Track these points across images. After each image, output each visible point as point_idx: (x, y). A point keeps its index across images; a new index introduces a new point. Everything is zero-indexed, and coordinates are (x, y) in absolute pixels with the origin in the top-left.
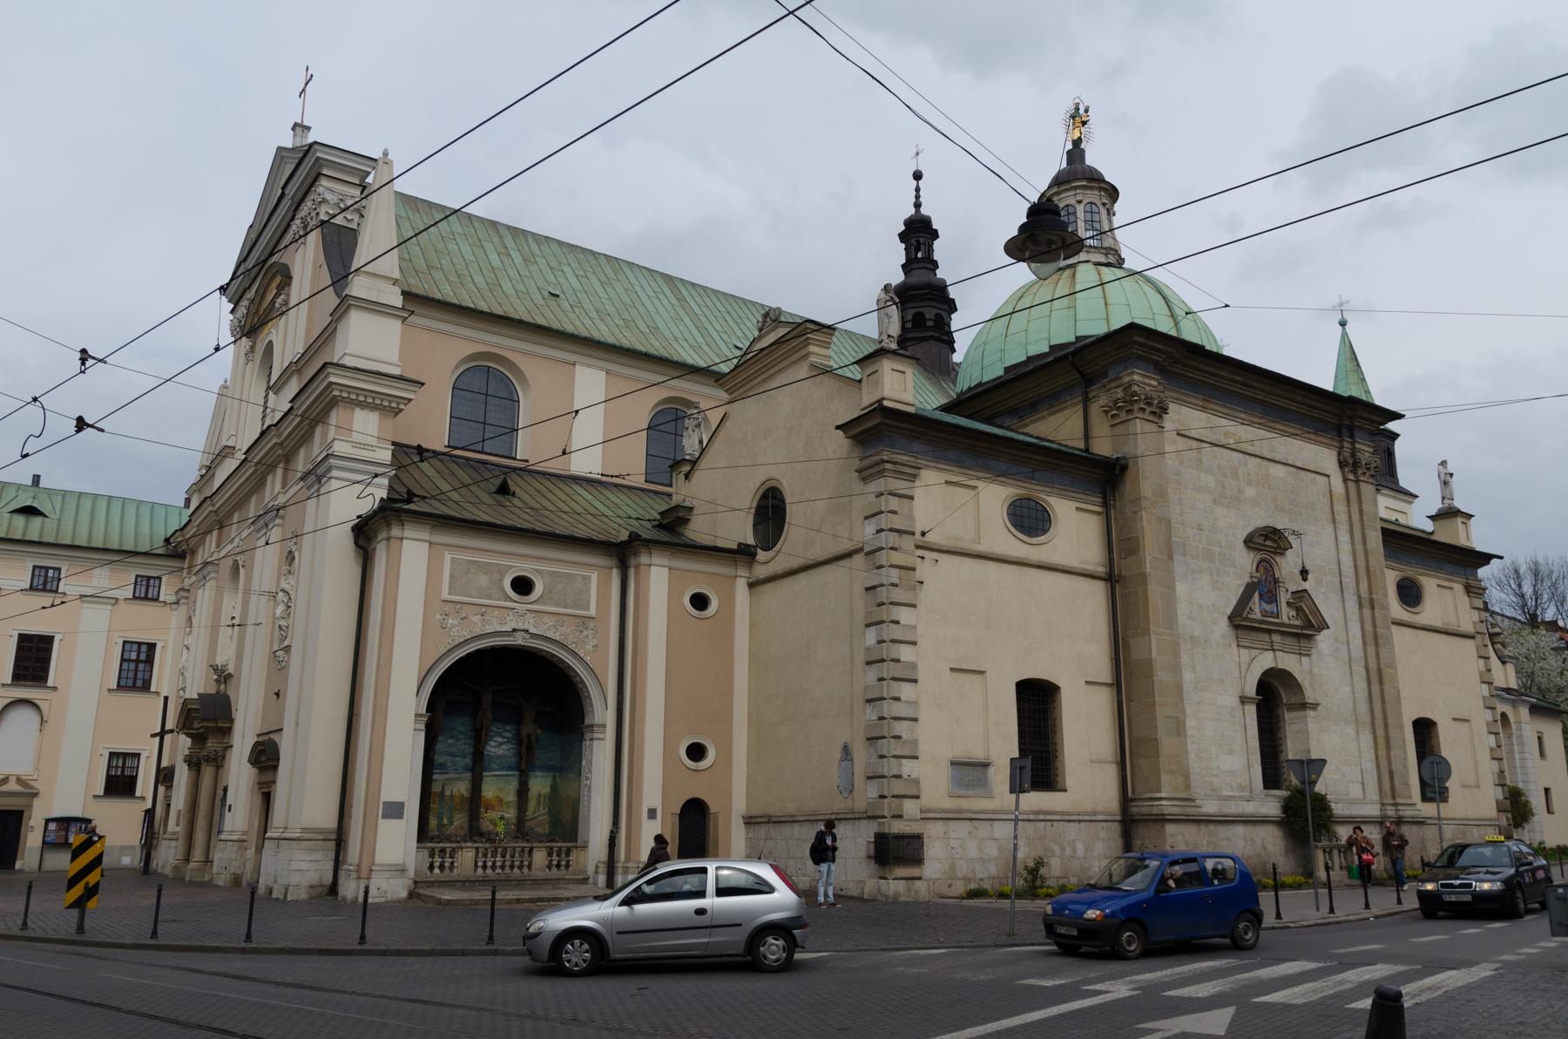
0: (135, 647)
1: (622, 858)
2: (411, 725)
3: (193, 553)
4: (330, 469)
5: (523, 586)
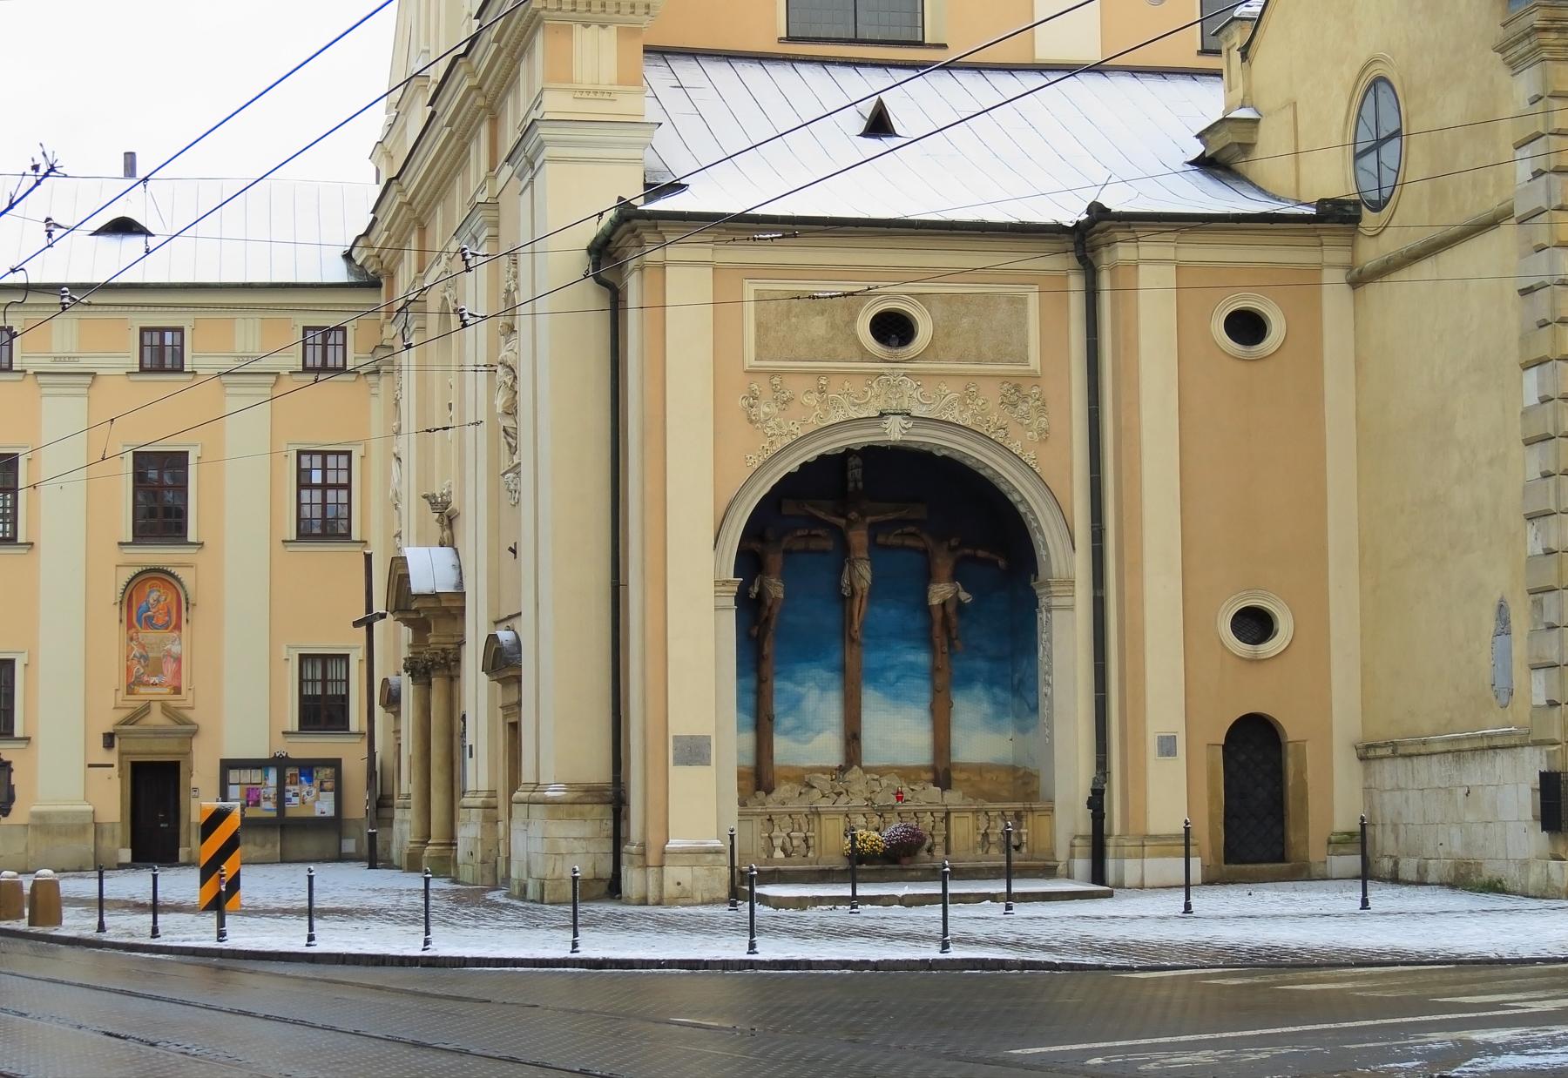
0: (317, 460)
1: (1117, 830)
2: (709, 600)
3: (392, 276)
4: (541, 146)
5: (893, 329)
